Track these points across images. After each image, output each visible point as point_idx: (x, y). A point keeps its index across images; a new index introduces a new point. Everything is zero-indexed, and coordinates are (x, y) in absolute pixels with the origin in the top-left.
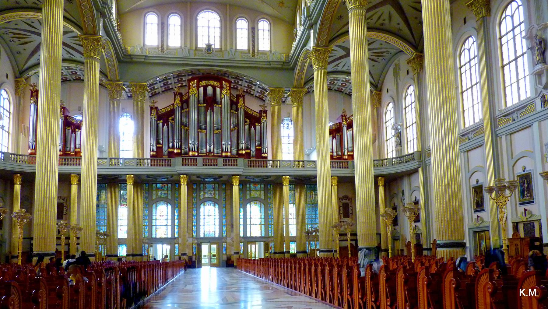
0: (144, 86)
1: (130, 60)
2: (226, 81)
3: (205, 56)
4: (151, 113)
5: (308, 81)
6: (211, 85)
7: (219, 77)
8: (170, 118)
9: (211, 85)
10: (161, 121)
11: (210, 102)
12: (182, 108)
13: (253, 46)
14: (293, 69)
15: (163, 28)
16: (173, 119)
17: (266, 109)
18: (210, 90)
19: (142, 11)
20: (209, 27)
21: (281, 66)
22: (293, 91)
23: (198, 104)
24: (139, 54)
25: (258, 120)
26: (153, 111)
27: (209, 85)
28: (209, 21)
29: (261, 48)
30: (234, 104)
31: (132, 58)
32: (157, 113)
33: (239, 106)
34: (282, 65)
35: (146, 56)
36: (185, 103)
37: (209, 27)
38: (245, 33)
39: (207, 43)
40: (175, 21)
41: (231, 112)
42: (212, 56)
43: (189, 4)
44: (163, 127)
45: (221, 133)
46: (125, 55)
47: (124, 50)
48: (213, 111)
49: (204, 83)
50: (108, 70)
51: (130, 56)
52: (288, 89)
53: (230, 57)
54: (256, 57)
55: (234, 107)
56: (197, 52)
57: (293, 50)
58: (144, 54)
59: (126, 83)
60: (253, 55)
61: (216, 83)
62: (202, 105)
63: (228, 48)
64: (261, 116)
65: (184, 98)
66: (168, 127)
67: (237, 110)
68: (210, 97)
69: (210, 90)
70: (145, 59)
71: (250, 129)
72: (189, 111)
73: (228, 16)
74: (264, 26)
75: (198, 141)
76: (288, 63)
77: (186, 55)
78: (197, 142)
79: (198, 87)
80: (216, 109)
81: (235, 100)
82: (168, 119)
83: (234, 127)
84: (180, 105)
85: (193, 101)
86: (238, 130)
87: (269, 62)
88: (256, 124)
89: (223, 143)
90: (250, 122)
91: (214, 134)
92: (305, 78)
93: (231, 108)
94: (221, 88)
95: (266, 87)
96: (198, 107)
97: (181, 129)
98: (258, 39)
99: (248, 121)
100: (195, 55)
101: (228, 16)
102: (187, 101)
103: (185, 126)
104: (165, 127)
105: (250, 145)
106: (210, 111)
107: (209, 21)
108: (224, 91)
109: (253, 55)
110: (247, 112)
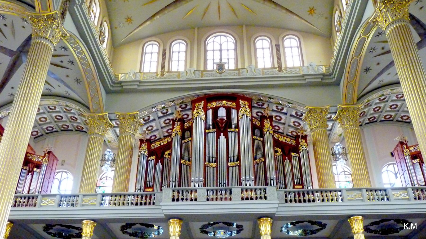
0: (134, 117)
1: (120, 89)
2: (244, 98)
3: (216, 76)
4: (140, 146)
5: (363, 96)
6: (224, 106)
7: (234, 97)
8: (166, 153)
9: (224, 106)
10: (154, 157)
11: (222, 127)
12: (183, 137)
13: (279, 63)
14: (337, 84)
15: (165, 55)
16: (170, 154)
17: (305, 133)
18: (222, 113)
19: (140, 40)
20: (221, 50)
21: (320, 80)
22: (343, 110)
23: (206, 129)
24: (131, 80)
25: (296, 149)
26: (143, 145)
27: (220, 107)
28: (221, 45)
29: (290, 64)
30: (257, 129)
31: (122, 86)
32: (149, 148)
33: (265, 130)
34: (322, 79)
35: (140, 82)
36: (187, 131)
37: (221, 50)
38: (268, 52)
39: (217, 61)
40: (179, 48)
41: (253, 139)
42: (225, 76)
43: (196, 29)
44: (156, 164)
45: (240, 166)
46: (113, 82)
47: (113, 77)
48: (227, 137)
49: (214, 104)
50: (90, 98)
51: (120, 83)
52: (333, 110)
53: (249, 74)
54: (285, 72)
55: (257, 132)
56: (204, 73)
57: (336, 52)
58: (139, 79)
59: (113, 117)
60: (280, 69)
61: (229, 104)
62: (211, 131)
63: (246, 66)
64: (298, 143)
65: (186, 125)
66: (163, 164)
67: (262, 135)
68: (222, 120)
69: (222, 113)
70: (138, 86)
71: (284, 161)
72: (191, 141)
73: (244, 34)
74: (291, 44)
75: (205, 178)
76: (330, 75)
77: (192, 76)
78: (202, 179)
79: (205, 109)
80: (230, 135)
81: (258, 124)
82: (163, 154)
83: (259, 158)
84: (179, 133)
85: (199, 127)
86: (265, 162)
87: (303, 76)
88: (292, 154)
89: (243, 178)
90: (283, 151)
91: (228, 167)
92: (358, 92)
93: (253, 134)
94: (238, 108)
95: (301, 109)
96: (205, 134)
97: (181, 165)
98: (285, 57)
99: (279, 150)
100: (202, 76)
101: (244, 34)
102: (190, 129)
103: (186, 160)
104: (159, 165)
105: (285, 184)
106: (222, 138)
107: (221, 45)
108: (241, 112)
109: (280, 69)
110: (278, 140)
